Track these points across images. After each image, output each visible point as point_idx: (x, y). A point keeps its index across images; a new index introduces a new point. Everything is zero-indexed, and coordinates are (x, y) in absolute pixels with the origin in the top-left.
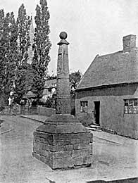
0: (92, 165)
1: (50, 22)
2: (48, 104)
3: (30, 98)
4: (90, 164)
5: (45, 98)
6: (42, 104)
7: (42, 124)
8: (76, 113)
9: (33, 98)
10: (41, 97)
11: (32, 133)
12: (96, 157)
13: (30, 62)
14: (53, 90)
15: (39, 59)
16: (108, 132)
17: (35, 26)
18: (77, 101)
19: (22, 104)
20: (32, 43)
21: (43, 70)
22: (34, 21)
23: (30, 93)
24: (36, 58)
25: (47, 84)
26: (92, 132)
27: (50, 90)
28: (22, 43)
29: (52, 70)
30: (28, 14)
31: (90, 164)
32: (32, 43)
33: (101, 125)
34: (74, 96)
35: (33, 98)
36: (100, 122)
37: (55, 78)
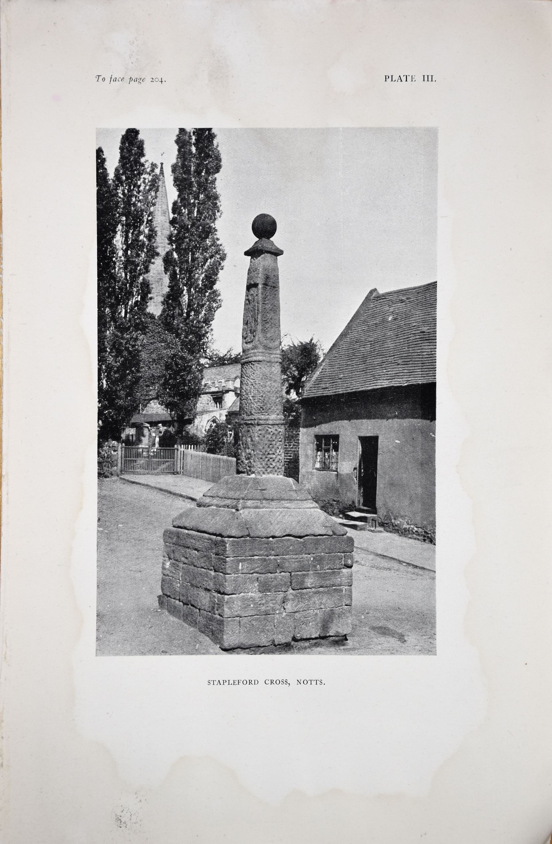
0: (350, 642)
1: (222, 183)
2: (213, 443)
3: (154, 424)
4: (345, 638)
5: (201, 426)
6: (192, 441)
7: (193, 505)
8: (302, 471)
9: (164, 423)
10: (190, 421)
11: (160, 533)
12: (364, 610)
13: (155, 308)
14: (230, 399)
15: (185, 299)
16: (404, 533)
17: (172, 194)
18: (306, 436)
19: (128, 442)
20: (163, 246)
21: (195, 339)
22: (169, 178)
23: (155, 409)
24: (173, 296)
25: (212, 379)
26: (351, 533)
27: (218, 398)
28: (128, 247)
29: (225, 333)
30: (150, 157)
31: (345, 638)
32: (163, 246)
33: (382, 512)
34: (297, 418)
35: (164, 423)
36: (379, 503)
37: (235, 361)
